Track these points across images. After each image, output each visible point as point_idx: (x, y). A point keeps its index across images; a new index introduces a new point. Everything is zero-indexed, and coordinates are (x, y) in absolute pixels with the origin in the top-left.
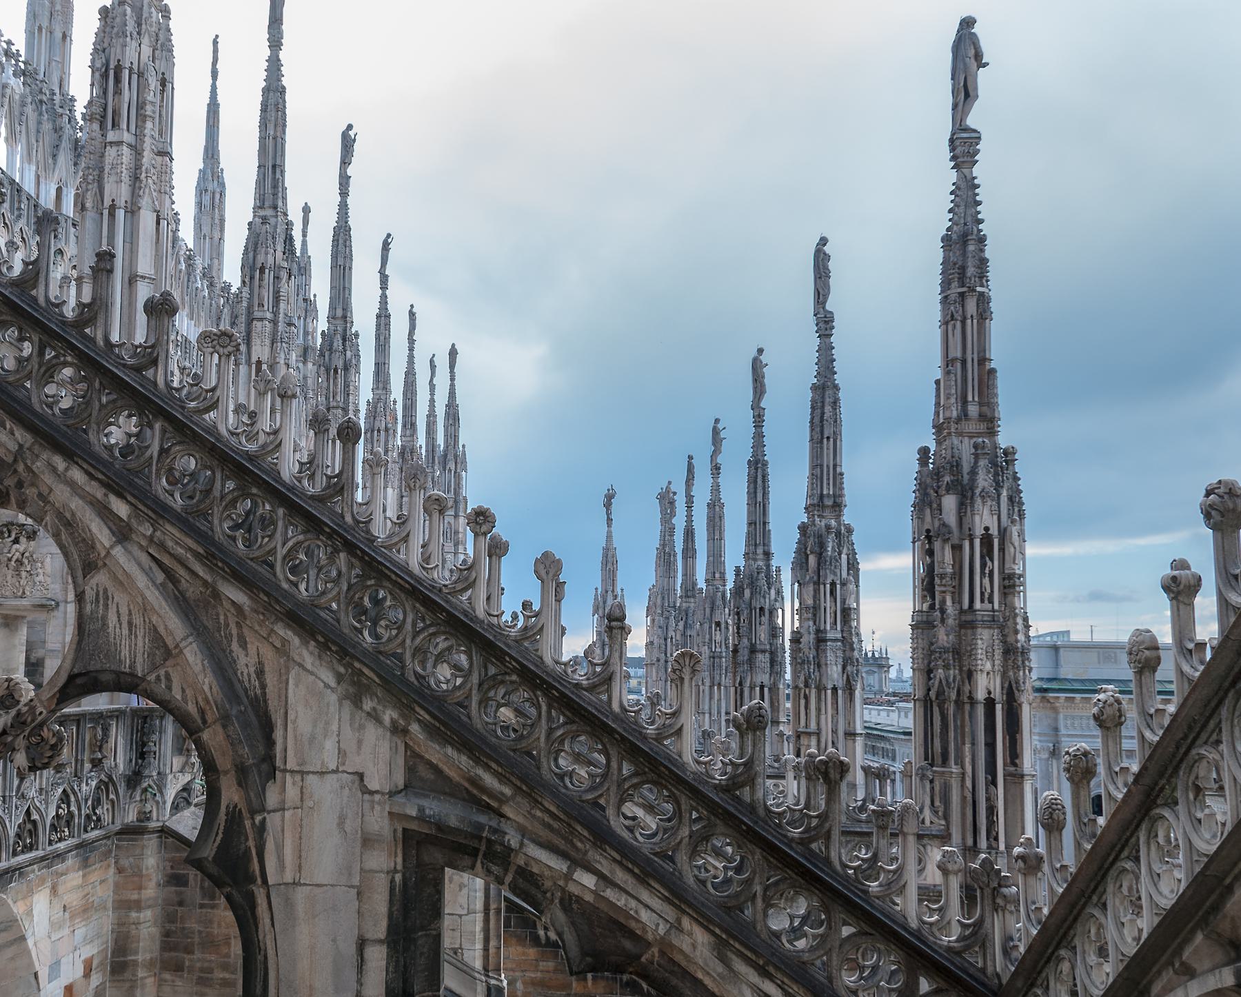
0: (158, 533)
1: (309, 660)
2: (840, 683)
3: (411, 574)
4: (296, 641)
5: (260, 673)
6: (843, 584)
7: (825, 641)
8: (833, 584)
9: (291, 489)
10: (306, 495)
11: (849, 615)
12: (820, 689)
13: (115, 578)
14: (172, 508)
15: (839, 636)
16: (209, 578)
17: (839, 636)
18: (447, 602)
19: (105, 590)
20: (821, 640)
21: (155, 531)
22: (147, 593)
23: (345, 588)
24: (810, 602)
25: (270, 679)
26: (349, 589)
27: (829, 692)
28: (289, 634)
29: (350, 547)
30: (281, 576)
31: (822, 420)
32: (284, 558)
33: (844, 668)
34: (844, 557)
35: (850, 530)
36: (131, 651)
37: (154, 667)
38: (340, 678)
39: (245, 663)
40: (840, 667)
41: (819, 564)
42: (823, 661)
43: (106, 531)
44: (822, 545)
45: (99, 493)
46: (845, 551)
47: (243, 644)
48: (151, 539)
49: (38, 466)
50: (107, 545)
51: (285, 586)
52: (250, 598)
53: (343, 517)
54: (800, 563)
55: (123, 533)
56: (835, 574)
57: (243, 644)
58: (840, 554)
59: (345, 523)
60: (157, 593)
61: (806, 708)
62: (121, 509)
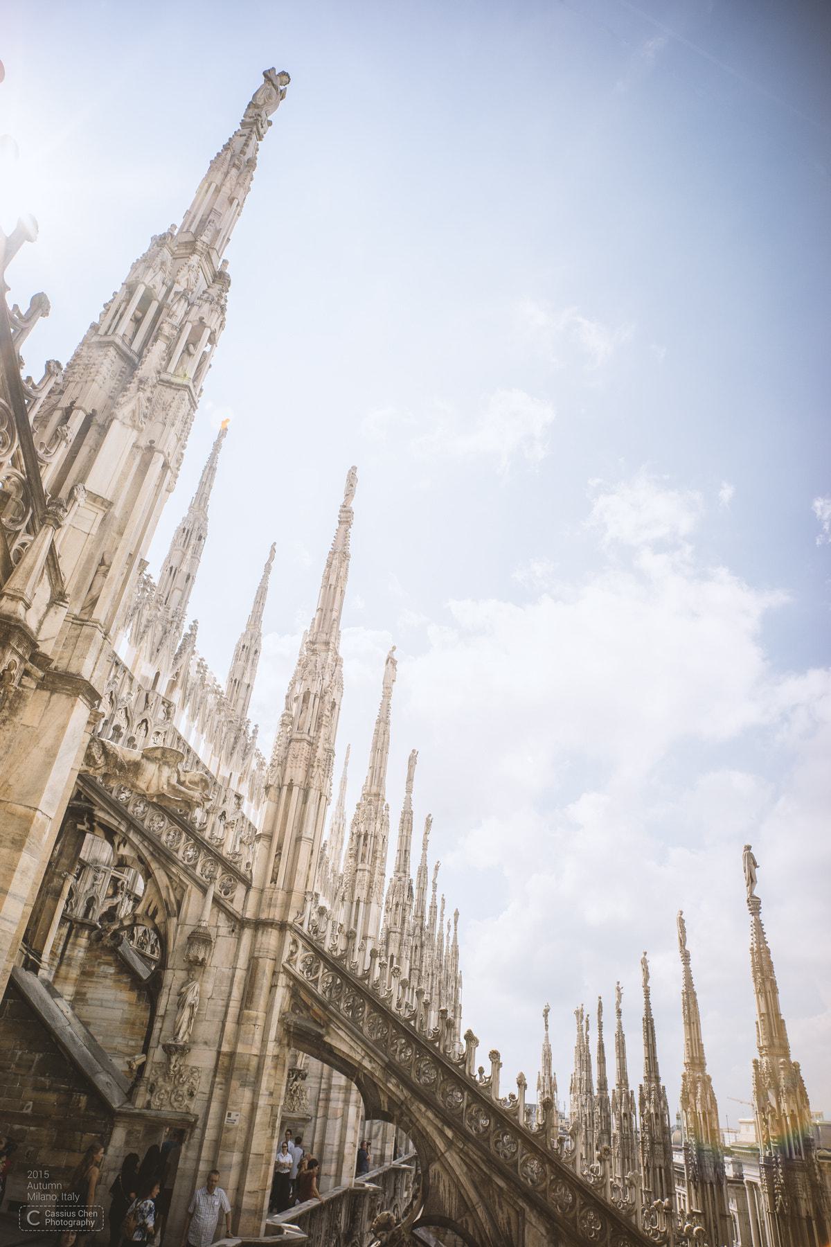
1: (533, 1220)
2: (714, 1180)
4: (528, 1209)
5: (509, 1223)
9: (524, 1130)
12: (703, 1182)
13: (443, 1166)
24: (691, 1126)
25: (513, 1227)
28: (524, 1205)
29: (551, 1162)
35: (710, 1080)
36: (450, 1205)
37: (460, 1216)
38: (548, 1231)
39: (502, 1217)
44: (696, 1088)
47: (501, 1207)
49: (413, 1108)
54: (685, 1101)
55: (450, 1144)
57: (501, 1207)
62: (449, 1134)
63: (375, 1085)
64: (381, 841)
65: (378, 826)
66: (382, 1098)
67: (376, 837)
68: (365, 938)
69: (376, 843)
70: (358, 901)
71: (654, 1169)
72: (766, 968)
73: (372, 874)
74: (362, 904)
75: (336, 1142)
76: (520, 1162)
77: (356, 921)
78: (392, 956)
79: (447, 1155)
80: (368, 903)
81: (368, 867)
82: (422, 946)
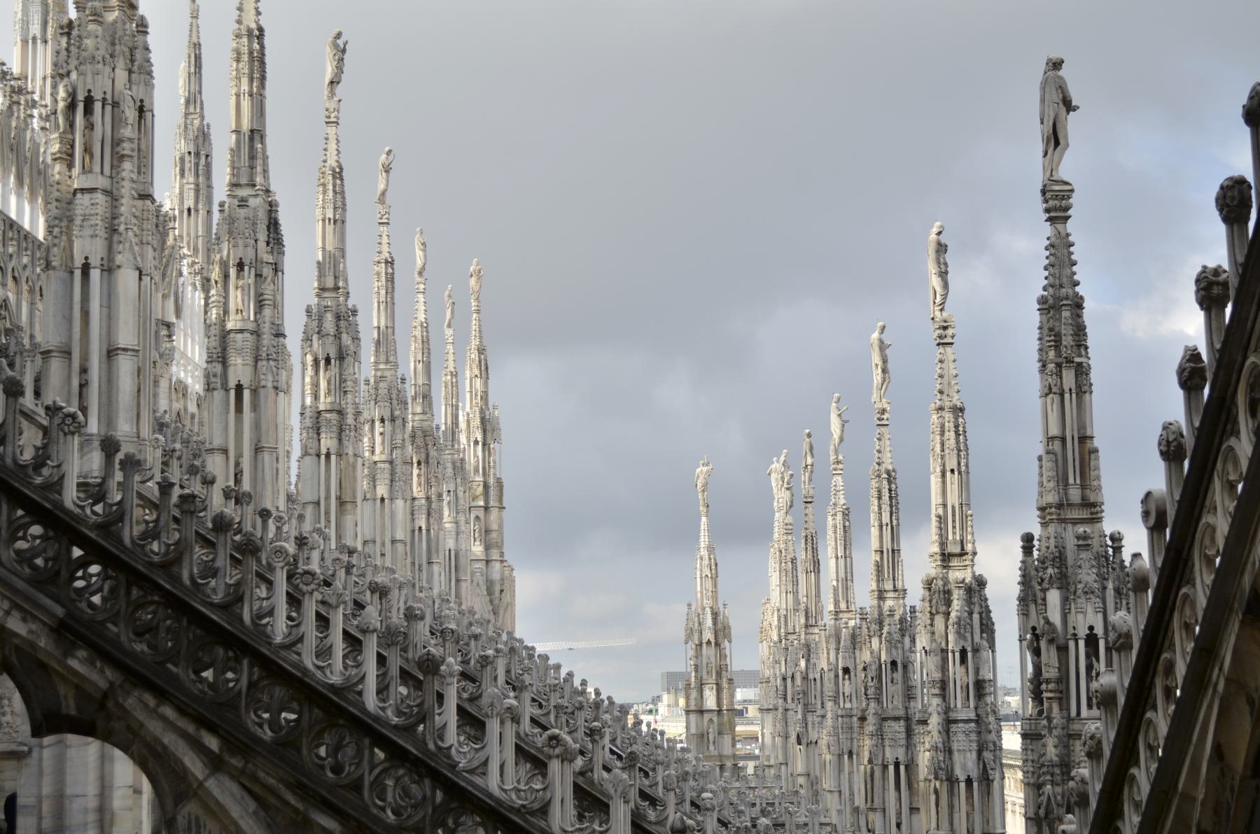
0: (250, 765)
2: (974, 774)
3: (491, 796)
6: (976, 650)
7: (956, 721)
8: (963, 653)
9: (376, 719)
10: (389, 725)
11: (984, 688)
12: (952, 781)
14: (261, 739)
15: (972, 716)
16: (300, 806)
17: (972, 716)
18: (526, 821)
19: (197, 819)
20: (948, 722)
21: (247, 762)
22: (242, 823)
23: (430, 811)
26: (434, 811)
27: (963, 785)
30: (370, 803)
31: (943, 450)
32: (372, 784)
33: (980, 753)
34: (976, 616)
40: (974, 755)
41: (947, 627)
42: (955, 746)
43: (199, 764)
44: (948, 603)
45: (191, 728)
46: (977, 609)
48: (242, 772)
50: (200, 777)
51: (375, 811)
52: (341, 823)
53: (426, 744)
55: (215, 764)
56: (965, 639)
58: (971, 613)
59: (428, 750)
60: (251, 822)
61: (937, 805)
62: (213, 743)
63: (43, 666)
64: (131, 114)
65: (121, 75)
66: (62, 689)
67: (115, 105)
68: (111, 353)
69: (117, 122)
70: (86, 268)
71: (885, 767)
72: (1067, 340)
73: (112, 196)
74: (95, 274)
75: (92, 789)
76: (367, 780)
77: (85, 314)
78: (239, 388)
79: (211, 784)
80: (109, 269)
81: (102, 182)
82: (341, 358)
